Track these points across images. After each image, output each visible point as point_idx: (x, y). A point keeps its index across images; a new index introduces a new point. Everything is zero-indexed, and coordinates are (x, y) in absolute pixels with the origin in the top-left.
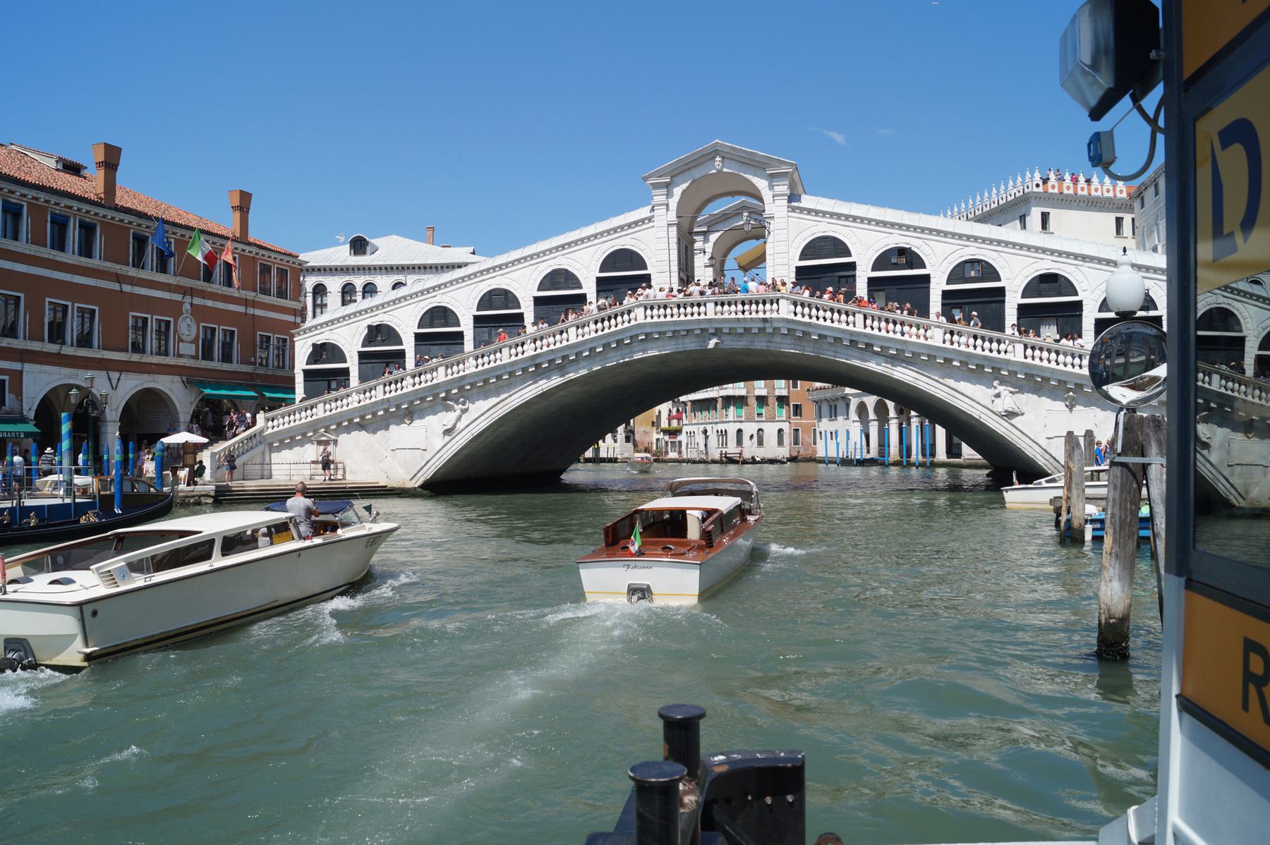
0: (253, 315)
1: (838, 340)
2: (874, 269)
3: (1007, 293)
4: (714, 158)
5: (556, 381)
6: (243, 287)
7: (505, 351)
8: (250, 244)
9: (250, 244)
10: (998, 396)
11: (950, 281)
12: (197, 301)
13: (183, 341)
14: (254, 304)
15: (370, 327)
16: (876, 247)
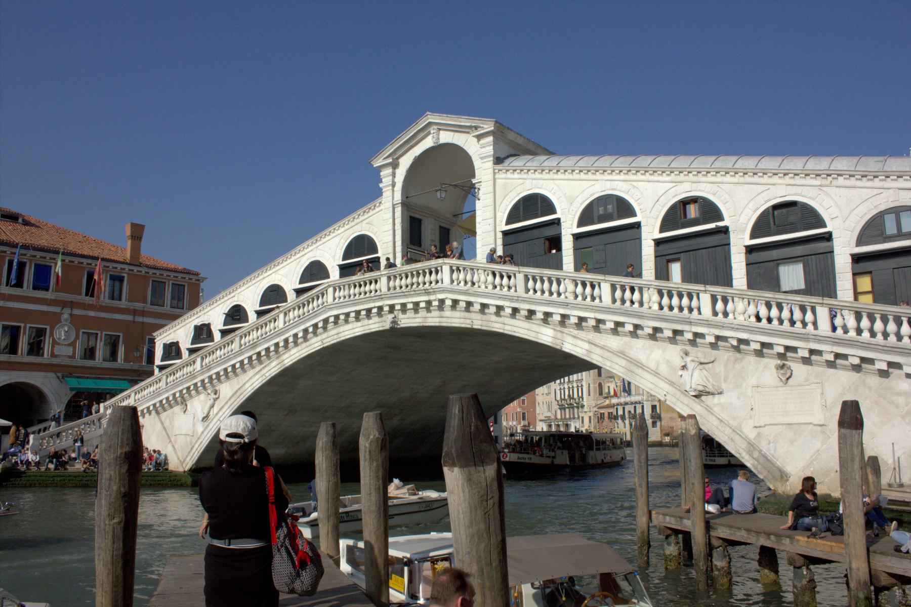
0: (143, 323)
1: (500, 308)
2: (581, 224)
3: (732, 235)
4: (429, 133)
5: (272, 369)
6: (130, 300)
7: (237, 339)
8: (140, 265)
9: (140, 265)
10: (684, 367)
11: (664, 228)
12: (77, 312)
13: (58, 344)
14: (143, 313)
15: (196, 327)
16: (580, 199)
